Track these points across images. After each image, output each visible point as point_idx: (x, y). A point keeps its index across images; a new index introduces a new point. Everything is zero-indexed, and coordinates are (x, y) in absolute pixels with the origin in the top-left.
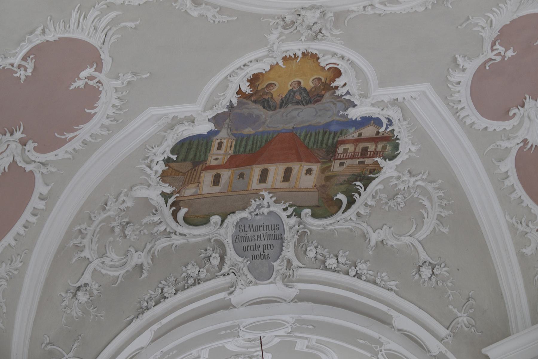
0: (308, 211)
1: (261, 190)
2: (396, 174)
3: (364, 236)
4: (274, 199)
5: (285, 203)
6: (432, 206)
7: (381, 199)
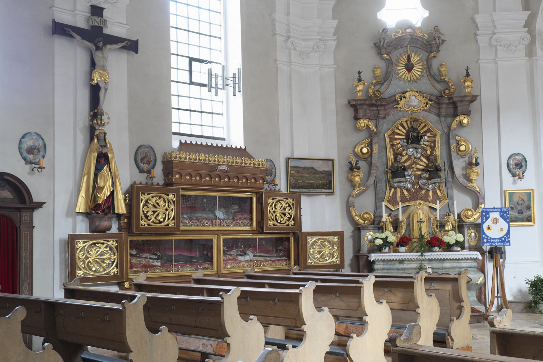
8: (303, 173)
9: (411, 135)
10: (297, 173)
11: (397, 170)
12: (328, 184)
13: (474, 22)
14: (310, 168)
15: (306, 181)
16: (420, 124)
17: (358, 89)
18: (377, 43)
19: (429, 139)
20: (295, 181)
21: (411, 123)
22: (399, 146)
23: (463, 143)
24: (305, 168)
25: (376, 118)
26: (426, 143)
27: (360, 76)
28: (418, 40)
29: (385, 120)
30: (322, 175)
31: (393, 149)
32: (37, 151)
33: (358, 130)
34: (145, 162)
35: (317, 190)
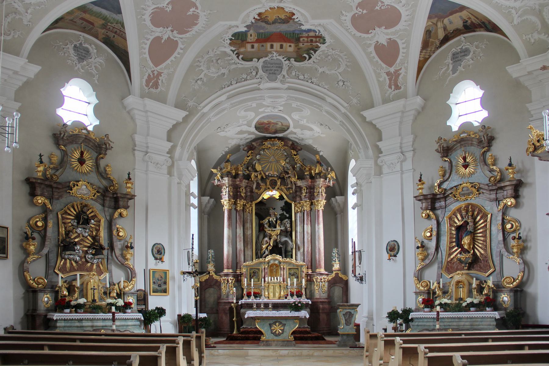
0: (293, 59)
1: (272, 51)
2: (326, 49)
3: (316, 69)
4: (278, 54)
5: (283, 56)
6: (343, 61)
7: (322, 57)
9: (83, 217)
11: (69, 245)
13: (133, 140)
16: (89, 210)
17: (39, 169)
18: (58, 134)
19: (95, 223)
21: (81, 207)
22: (70, 224)
23: (121, 230)
25: (51, 198)
26: (93, 226)
27: (41, 159)
28: (90, 141)
29: (58, 201)
31: (65, 226)
33: (33, 204)
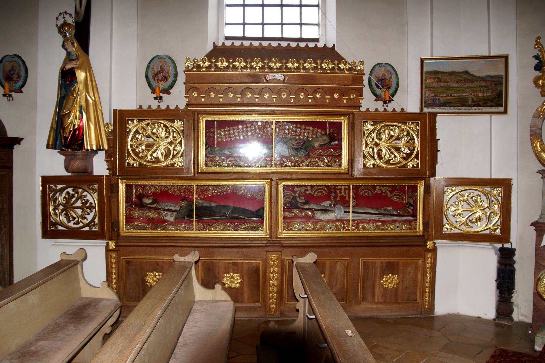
8: (447, 82)
10: (438, 82)
12: (495, 98)
14: (462, 72)
15: (453, 95)
20: (432, 95)
24: (452, 73)
30: (484, 84)
32: (17, 76)
34: (160, 79)
35: (473, 108)
